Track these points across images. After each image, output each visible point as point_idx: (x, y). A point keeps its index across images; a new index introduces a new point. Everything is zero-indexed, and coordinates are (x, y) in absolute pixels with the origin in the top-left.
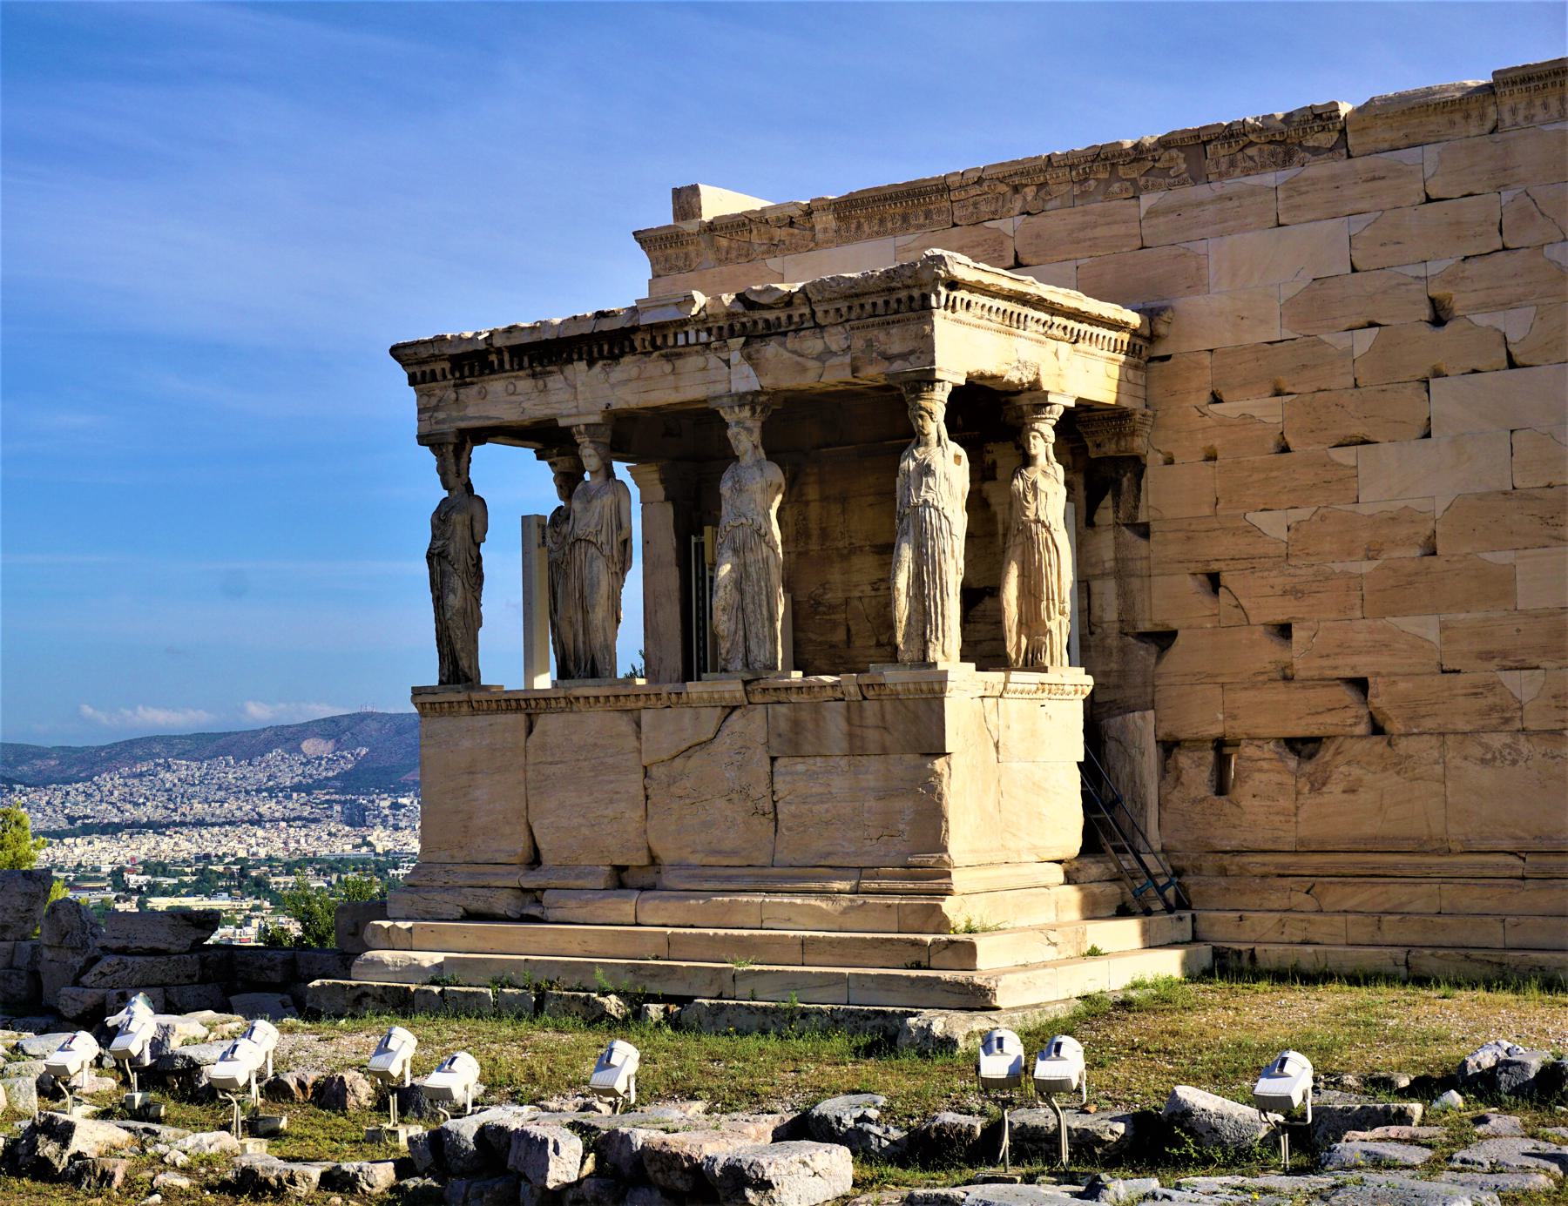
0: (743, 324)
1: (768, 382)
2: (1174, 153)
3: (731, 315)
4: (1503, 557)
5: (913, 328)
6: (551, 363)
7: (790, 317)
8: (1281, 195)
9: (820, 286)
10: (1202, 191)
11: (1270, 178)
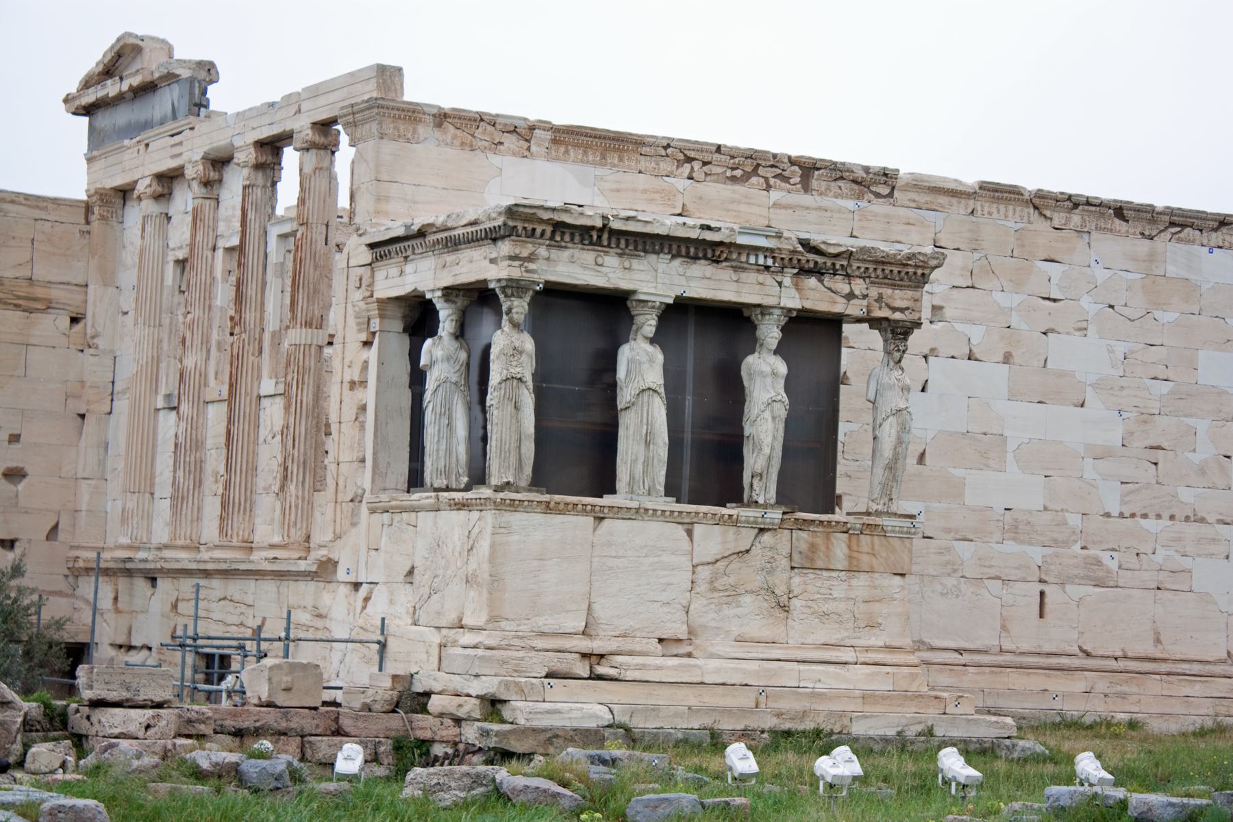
0: (799, 260)
1: (808, 305)
2: (796, 168)
3: (794, 252)
4: (959, 472)
5: (909, 293)
6: (645, 251)
7: (834, 264)
8: (856, 218)
9: (863, 250)
10: (806, 199)
11: (850, 204)
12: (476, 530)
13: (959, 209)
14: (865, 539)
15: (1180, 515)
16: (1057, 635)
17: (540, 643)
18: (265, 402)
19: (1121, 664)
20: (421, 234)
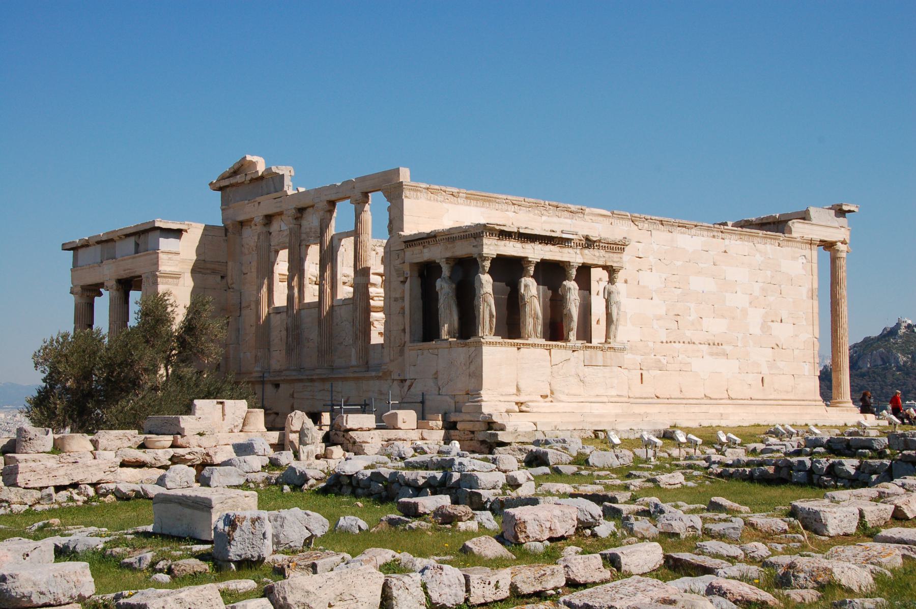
1: (586, 261)
5: (619, 255)
10: (555, 219)
11: (569, 221)
12: (473, 355)
13: (607, 222)
14: (608, 353)
15: (686, 342)
16: (648, 390)
17: (502, 399)
18: (336, 308)
19: (670, 401)
20: (435, 236)
